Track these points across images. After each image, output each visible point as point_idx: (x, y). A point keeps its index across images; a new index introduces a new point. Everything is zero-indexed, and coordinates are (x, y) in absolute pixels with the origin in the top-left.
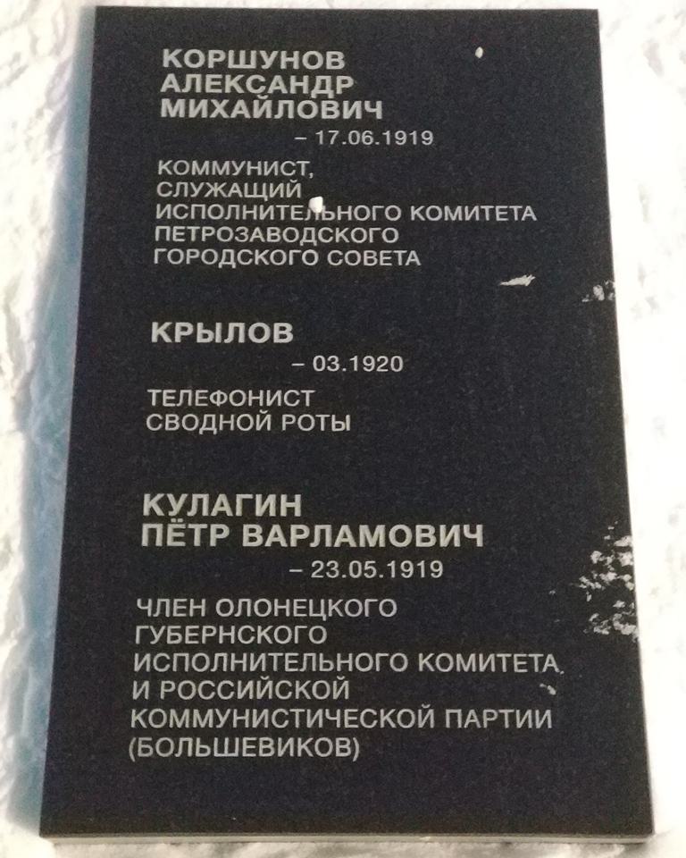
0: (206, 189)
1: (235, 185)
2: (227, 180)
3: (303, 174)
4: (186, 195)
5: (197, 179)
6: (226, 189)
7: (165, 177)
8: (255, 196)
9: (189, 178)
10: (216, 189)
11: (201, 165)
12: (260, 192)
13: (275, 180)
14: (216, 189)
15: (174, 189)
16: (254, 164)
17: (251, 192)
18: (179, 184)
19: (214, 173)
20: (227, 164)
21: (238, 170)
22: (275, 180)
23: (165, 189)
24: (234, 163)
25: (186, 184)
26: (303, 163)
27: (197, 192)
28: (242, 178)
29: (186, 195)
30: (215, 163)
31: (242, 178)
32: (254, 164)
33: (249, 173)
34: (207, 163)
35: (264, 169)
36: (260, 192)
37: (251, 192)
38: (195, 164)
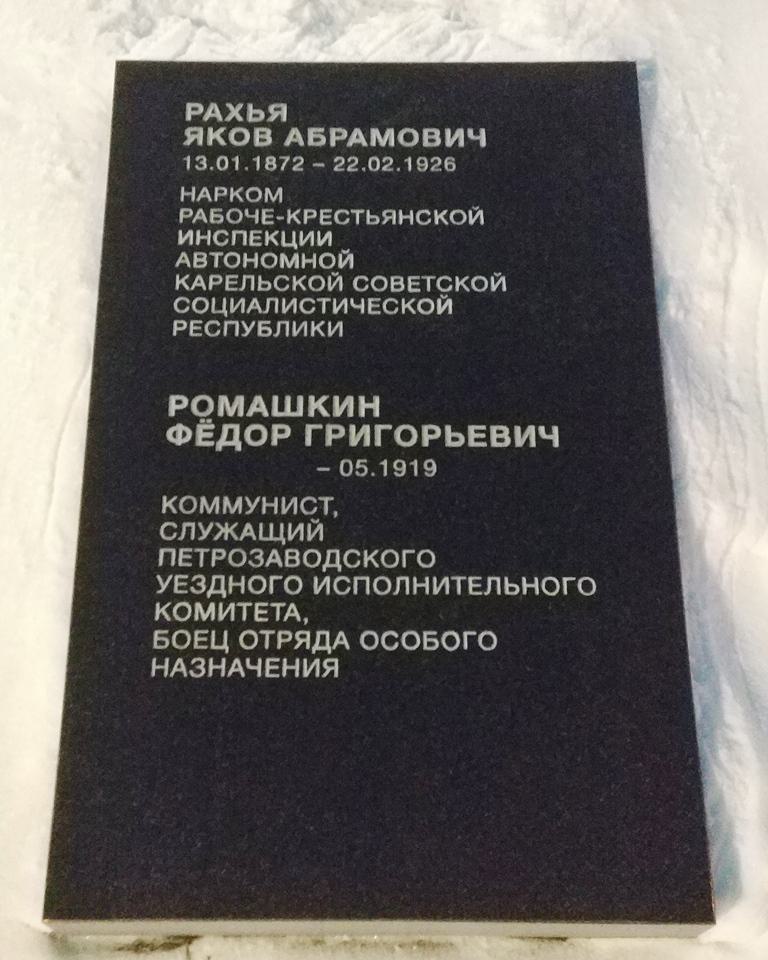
0: (215, 530)
1: (248, 526)
2: (240, 519)
3: (326, 512)
4: (193, 537)
5: (206, 518)
6: (239, 531)
7: (170, 516)
8: (271, 538)
9: (196, 517)
10: (226, 530)
11: (210, 502)
12: (276, 534)
13: (294, 519)
14: (226, 530)
15: (179, 530)
16: (270, 500)
17: (266, 534)
18: (185, 525)
19: (225, 511)
20: (239, 501)
21: (252, 507)
22: (294, 519)
23: (169, 531)
24: (247, 499)
25: (193, 525)
26: (326, 500)
27: (205, 534)
28: (256, 518)
29: (193, 537)
30: (227, 501)
31: (256, 518)
32: (270, 500)
33: (264, 511)
34: (217, 500)
35: (282, 506)
36: (276, 534)
37: (266, 534)
38: (203, 500)
